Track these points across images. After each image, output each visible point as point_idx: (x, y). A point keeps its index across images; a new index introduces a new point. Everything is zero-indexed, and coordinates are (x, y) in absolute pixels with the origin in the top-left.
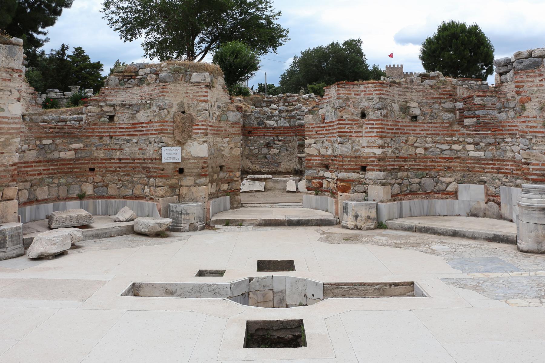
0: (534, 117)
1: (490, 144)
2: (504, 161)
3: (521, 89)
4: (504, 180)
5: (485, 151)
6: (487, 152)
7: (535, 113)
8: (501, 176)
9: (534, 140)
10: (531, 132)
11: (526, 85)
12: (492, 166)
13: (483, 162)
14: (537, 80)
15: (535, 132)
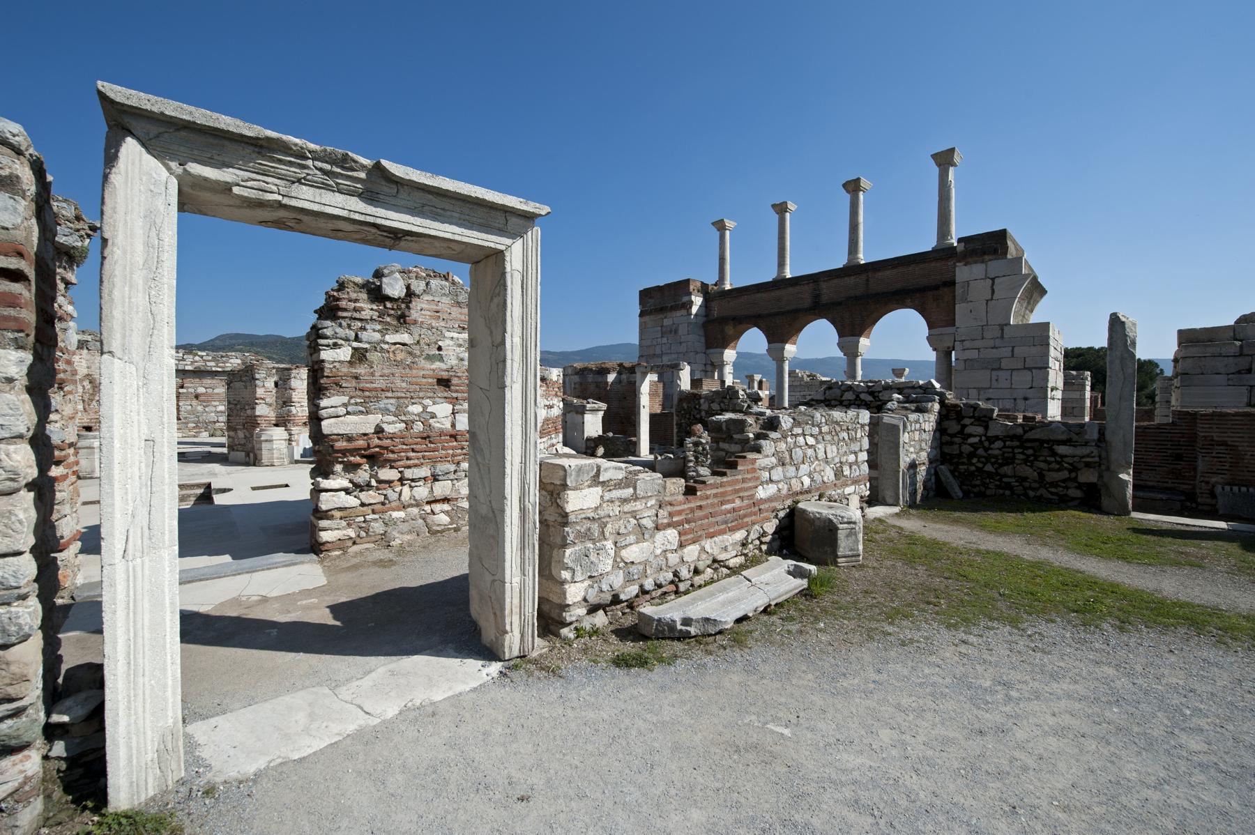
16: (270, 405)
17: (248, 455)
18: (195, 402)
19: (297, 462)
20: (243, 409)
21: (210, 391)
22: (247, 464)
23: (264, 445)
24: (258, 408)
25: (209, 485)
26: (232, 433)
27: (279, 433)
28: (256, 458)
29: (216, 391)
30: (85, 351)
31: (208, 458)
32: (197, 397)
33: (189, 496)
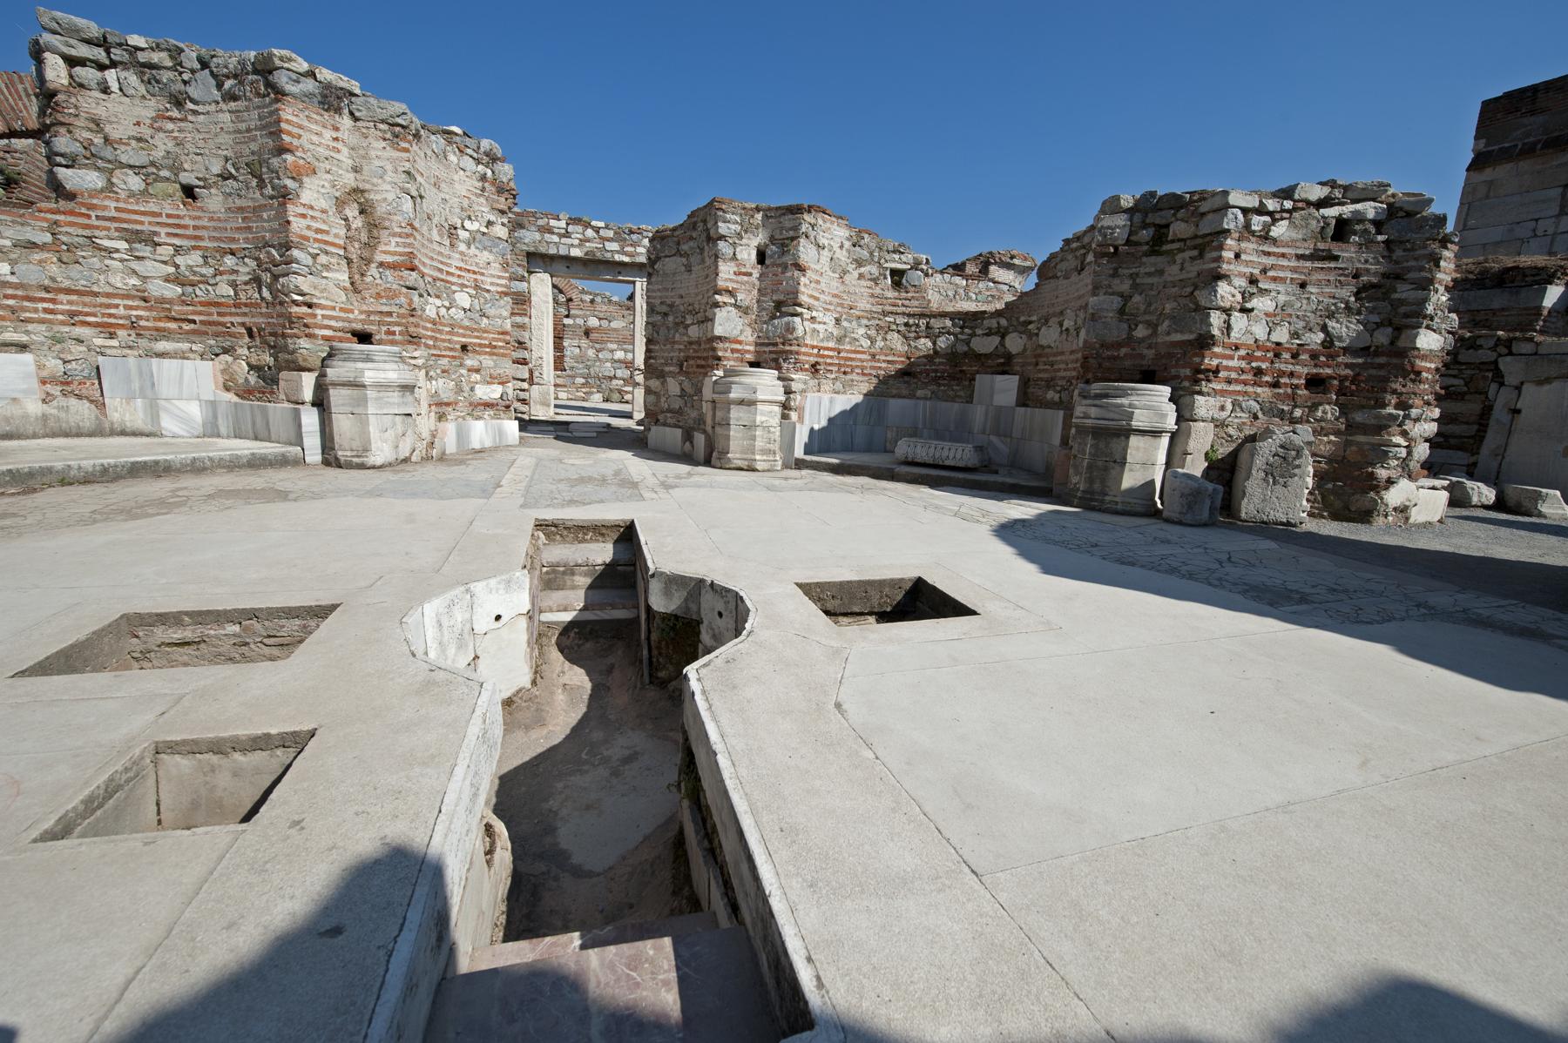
0: (324, 211)
1: (33, 246)
2: (96, 294)
3: (295, 142)
4: (99, 341)
5: (13, 263)
6: (21, 268)
7: (323, 204)
8: (79, 331)
9: (323, 259)
10: (316, 240)
11: (306, 136)
12: (45, 305)
13: (10, 292)
14: (328, 134)
15: (326, 243)
16: (745, 311)
17: (688, 437)
18: (584, 342)
19: (800, 464)
20: (681, 325)
21: (605, 323)
22: (687, 458)
23: (736, 414)
24: (720, 315)
25: (627, 536)
26: (655, 384)
27: (766, 383)
28: (710, 447)
29: (614, 325)
30: (346, 121)
31: (607, 437)
32: (587, 333)
33: (571, 570)
